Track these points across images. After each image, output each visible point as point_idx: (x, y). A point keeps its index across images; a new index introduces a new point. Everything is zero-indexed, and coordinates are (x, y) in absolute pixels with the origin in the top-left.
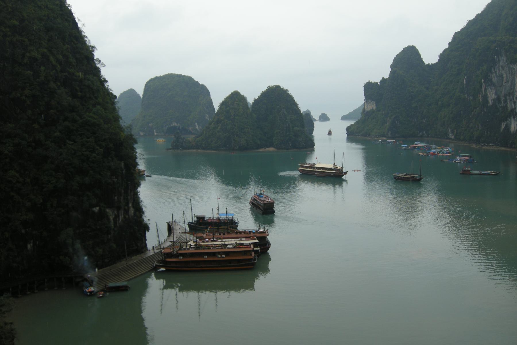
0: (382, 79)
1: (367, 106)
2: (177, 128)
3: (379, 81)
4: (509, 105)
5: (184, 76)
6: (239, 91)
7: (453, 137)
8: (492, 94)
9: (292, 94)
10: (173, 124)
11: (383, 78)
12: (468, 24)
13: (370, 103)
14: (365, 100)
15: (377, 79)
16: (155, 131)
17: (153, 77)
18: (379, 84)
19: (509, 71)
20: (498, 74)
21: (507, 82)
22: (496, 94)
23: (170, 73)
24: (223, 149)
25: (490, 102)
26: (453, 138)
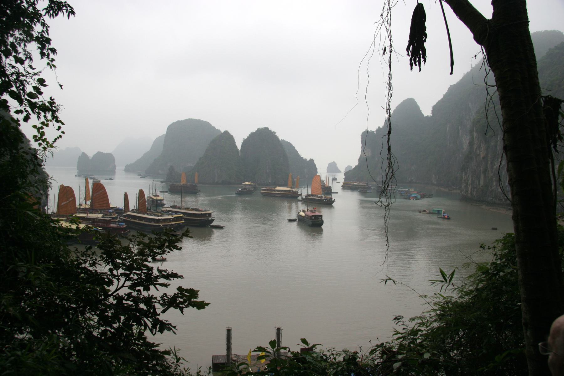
0: (378, 128)
3: (375, 130)
5: (203, 121)
6: (229, 131)
8: (467, 140)
9: (278, 136)
11: (379, 127)
14: (361, 147)
17: (175, 121)
18: (375, 132)
23: (191, 118)
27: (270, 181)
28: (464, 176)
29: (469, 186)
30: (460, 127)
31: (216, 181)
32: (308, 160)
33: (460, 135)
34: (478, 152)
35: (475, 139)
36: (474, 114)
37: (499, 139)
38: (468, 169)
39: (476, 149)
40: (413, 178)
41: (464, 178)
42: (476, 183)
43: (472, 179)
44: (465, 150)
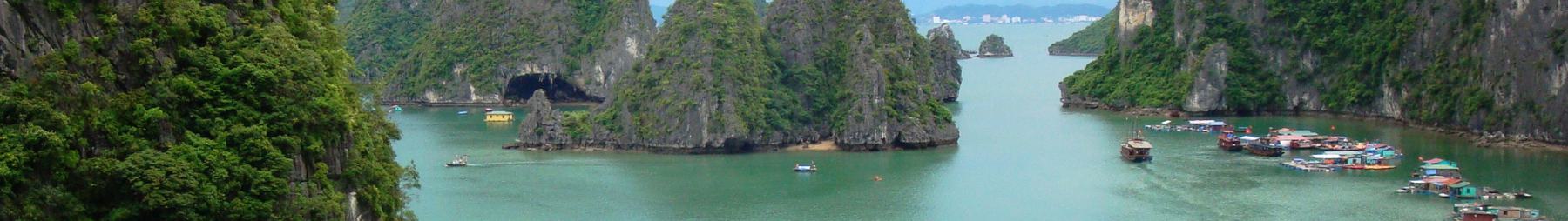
1: (1127, 14)
2: (541, 80)
7: (1397, 113)
10: (529, 70)
16: (472, 89)
24: (676, 146)
26: (1396, 117)
27: (883, 135)
31: (705, 141)
40: (1305, 98)
44: (1520, 9)
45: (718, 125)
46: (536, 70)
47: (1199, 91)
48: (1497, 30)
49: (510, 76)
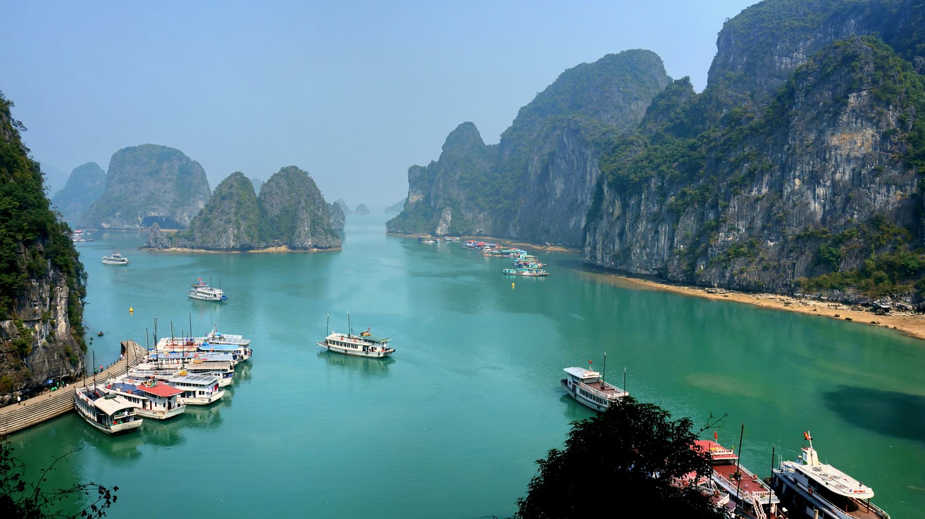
3: (428, 165)
4: (579, 197)
7: (515, 236)
11: (432, 161)
12: (537, 97)
13: (416, 192)
14: (409, 188)
15: (425, 163)
19: (580, 156)
20: (567, 160)
21: (578, 169)
22: (565, 183)
25: (559, 193)
26: (515, 237)
27: (309, 243)
28: (588, 238)
29: (598, 251)
30: (550, 167)
32: (332, 204)
33: (551, 177)
34: (611, 210)
35: (605, 193)
36: (570, 152)
37: (643, 197)
38: (597, 231)
39: (608, 205)
41: (588, 240)
42: (609, 247)
43: (603, 243)
44: (559, 196)
45: (237, 237)
46: (156, 214)
47: (440, 227)
48: (551, 202)
49: (144, 217)
